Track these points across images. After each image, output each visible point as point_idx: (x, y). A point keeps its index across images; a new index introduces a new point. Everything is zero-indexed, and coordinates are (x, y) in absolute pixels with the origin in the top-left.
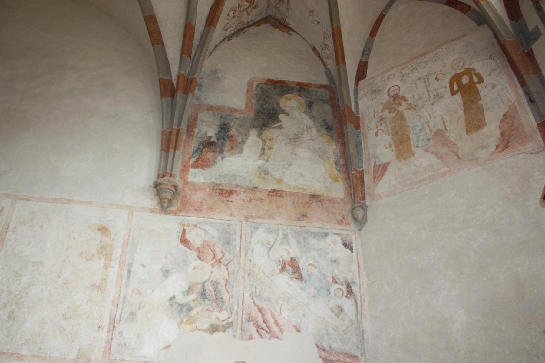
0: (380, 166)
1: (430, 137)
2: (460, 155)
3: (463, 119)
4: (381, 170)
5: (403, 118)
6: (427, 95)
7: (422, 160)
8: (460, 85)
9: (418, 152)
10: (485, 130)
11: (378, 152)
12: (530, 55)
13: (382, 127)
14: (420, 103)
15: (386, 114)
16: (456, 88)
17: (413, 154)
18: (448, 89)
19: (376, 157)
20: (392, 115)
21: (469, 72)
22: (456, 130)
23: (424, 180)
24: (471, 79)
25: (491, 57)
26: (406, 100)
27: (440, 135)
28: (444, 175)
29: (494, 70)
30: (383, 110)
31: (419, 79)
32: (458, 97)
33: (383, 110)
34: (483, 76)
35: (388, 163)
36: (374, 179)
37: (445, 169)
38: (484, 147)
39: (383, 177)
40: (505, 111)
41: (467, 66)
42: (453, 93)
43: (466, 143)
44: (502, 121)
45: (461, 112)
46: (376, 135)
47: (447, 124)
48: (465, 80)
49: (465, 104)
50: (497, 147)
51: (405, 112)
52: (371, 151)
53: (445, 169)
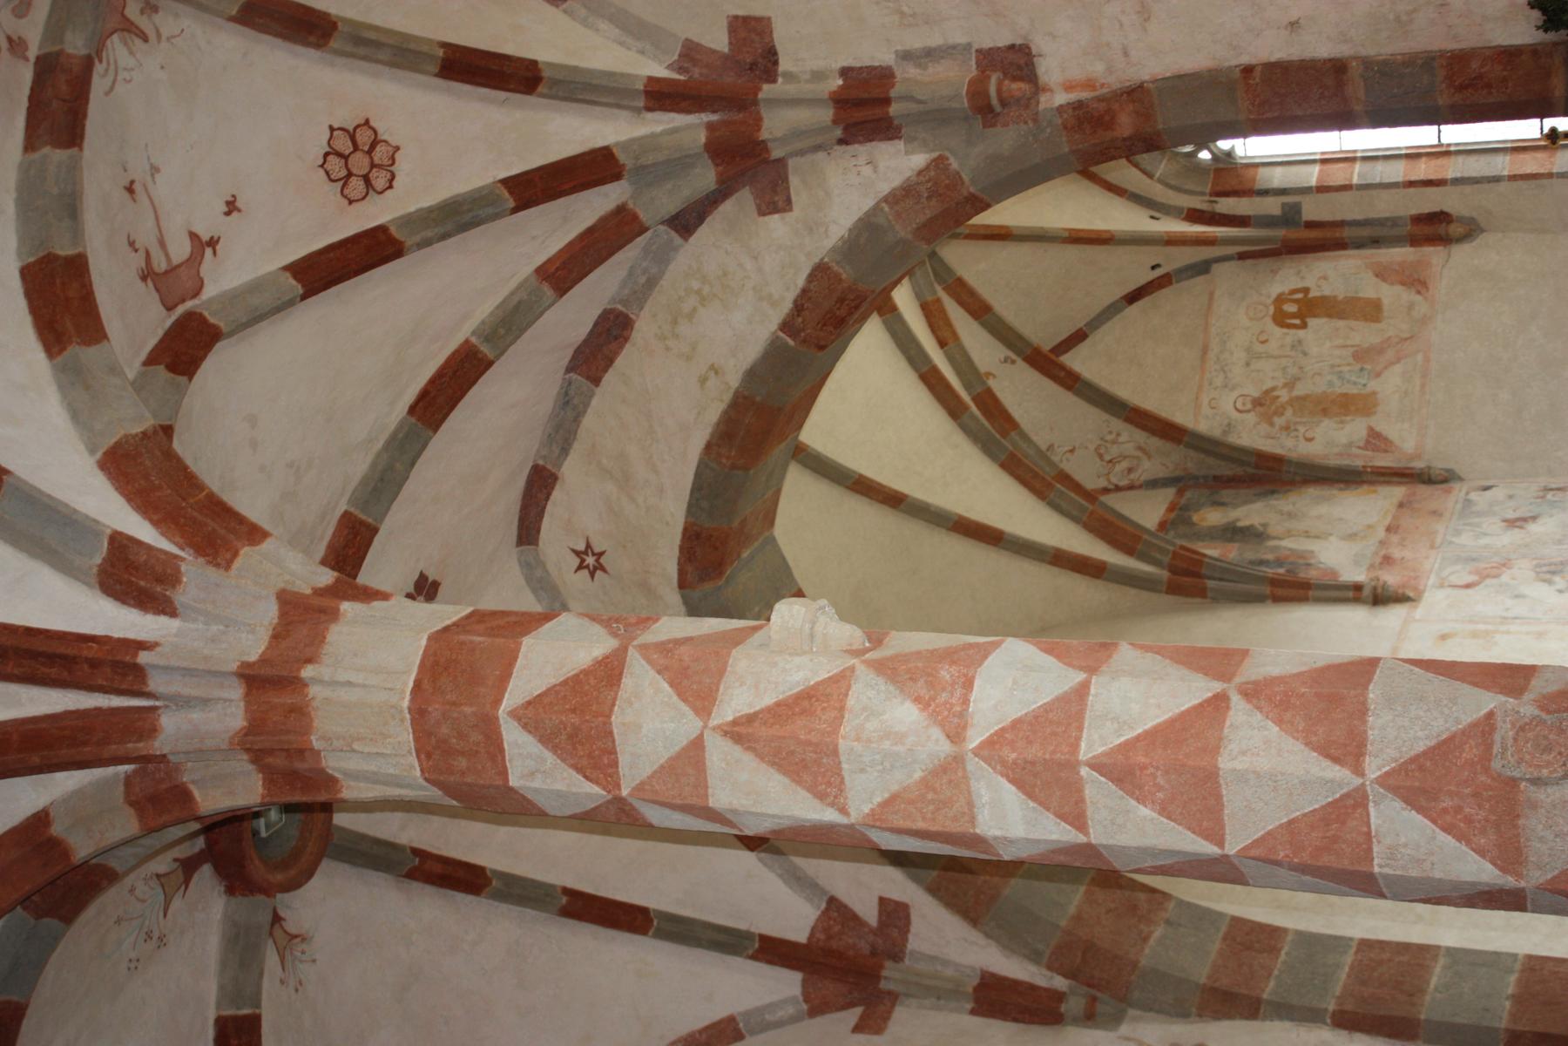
0: (1368, 442)
1: (1359, 366)
2: (1406, 335)
3: (1353, 323)
4: (1376, 440)
5: (1304, 398)
6: (1284, 361)
7: (1390, 385)
8: (1294, 316)
9: (1373, 385)
10: (1386, 302)
11: (1344, 440)
12: (1311, 225)
13: (1302, 429)
14: (1293, 371)
16: (1297, 322)
17: (1374, 393)
18: (1293, 331)
19: (1350, 445)
20: (1289, 412)
21: (1280, 300)
22: (1363, 334)
23: (1423, 386)
24: (1296, 301)
25: (1274, 272)
26: (1273, 389)
28: (1427, 360)
29: (1299, 272)
30: (1272, 424)
31: (1248, 364)
32: (1313, 322)
33: (1272, 424)
34: (1300, 285)
35: (1371, 429)
36: (1386, 451)
37: (1420, 357)
38: (1411, 307)
39: (1390, 437)
40: (1370, 274)
41: (1269, 301)
42: (1304, 326)
43: (1392, 326)
44: (1384, 280)
45: (1341, 323)
47: (1349, 342)
48: (1291, 308)
49: (1330, 316)
50: (1419, 292)
51: (1296, 393)
52: (1336, 450)
53: (1420, 357)
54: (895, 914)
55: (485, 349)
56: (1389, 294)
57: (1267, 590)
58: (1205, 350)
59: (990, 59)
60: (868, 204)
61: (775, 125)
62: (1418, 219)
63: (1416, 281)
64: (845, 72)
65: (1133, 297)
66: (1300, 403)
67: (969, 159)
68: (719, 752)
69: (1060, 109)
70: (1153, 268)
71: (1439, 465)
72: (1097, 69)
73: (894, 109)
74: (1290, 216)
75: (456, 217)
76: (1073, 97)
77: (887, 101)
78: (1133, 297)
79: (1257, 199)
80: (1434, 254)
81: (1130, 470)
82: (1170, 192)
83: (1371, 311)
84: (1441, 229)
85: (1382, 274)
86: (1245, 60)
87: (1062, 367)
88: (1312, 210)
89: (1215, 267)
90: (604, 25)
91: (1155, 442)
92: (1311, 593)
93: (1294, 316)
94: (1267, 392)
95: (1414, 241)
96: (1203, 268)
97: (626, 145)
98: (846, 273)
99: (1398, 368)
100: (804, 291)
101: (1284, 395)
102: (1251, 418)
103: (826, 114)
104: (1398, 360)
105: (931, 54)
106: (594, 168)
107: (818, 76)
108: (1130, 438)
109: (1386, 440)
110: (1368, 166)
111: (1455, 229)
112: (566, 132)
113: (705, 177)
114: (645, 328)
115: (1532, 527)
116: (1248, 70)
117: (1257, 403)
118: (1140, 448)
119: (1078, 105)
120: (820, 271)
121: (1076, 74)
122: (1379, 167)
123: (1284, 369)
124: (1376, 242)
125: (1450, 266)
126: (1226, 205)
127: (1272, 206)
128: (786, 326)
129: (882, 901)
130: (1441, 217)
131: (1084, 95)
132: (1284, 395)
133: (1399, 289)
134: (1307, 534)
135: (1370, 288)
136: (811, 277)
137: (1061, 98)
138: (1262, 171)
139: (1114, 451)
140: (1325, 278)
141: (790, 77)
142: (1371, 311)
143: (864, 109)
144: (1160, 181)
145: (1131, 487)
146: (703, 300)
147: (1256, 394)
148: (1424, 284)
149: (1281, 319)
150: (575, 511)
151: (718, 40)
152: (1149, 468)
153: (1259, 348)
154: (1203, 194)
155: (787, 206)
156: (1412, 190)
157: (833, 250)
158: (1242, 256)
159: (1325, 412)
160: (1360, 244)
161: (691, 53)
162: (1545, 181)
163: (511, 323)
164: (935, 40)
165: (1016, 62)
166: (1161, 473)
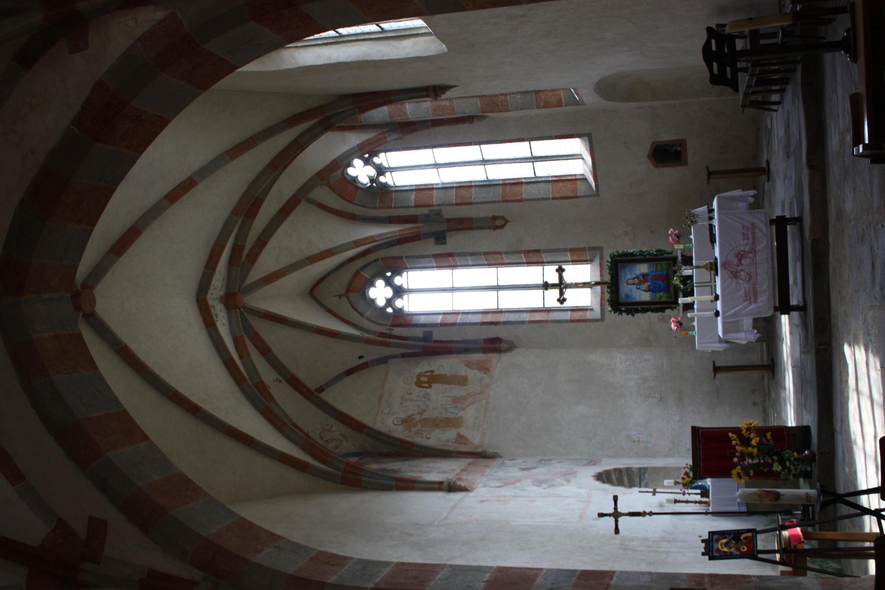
3: (453, 386)
4: (461, 439)
7: (469, 414)
8: (426, 382)
9: (461, 414)
10: (469, 377)
12: (436, 341)
13: (425, 433)
15: (414, 430)
17: (461, 417)
18: (424, 390)
19: (448, 441)
20: (419, 426)
21: (419, 375)
22: (458, 391)
23: (485, 414)
24: (427, 376)
26: (413, 415)
27: (456, 400)
28: (488, 403)
30: (410, 431)
32: (434, 386)
33: (410, 431)
34: (430, 369)
37: (484, 401)
38: (481, 379)
42: (430, 387)
44: (470, 368)
45: (448, 386)
46: (428, 438)
48: (425, 379)
49: (443, 383)
53: (484, 401)
54: (98, 527)
56: (471, 374)
57: (394, 483)
58: (381, 397)
62: (487, 341)
63: (485, 368)
65: (349, 372)
66: (424, 422)
70: (361, 357)
71: (490, 450)
74: (427, 337)
78: (349, 372)
79: (412, 329)
80: (493, 357)
81: (336, 447)
82: (371, 324)
83: (462, 381)
84: (497, 345)
85: (468, 365)
88: (438, 335)
89: (390, 361)
91: (349, 432)
92: (416, 485)
93: (426, 382)
94: (409, 417)
95: (485, 351)
96: (384, 360)
99: (474, 407)
101: (418, 418)
102: (400, 428)
104: (474, 403)
109: (466, 439)
110: (465, 316)
111: (504, 346)
115: (534, 471)
117: (404, 421)
118: (342, 435)
122: (470, 316)
123: (419, 406)
124: (467, 351)
125: (500, 362)
126: (397, 331)
127: (419, 332)
129: (91, 519)
130: (497, 340)
132: (418, 418)
133: (476, 372)
134: (421, 472)
135: (462, 371)
138: (415, 317)
140: (442, 366)
142: (462, 381)
144: (367, 318)
147: (404, 417)
148: (488, 370)
149: (419, 384)
153: (408, 396)
154: (387, 325)
156: (484, 326)
158: (404, 356)
159: (437, 426)
160: (459, 352)
162: (545, 324)
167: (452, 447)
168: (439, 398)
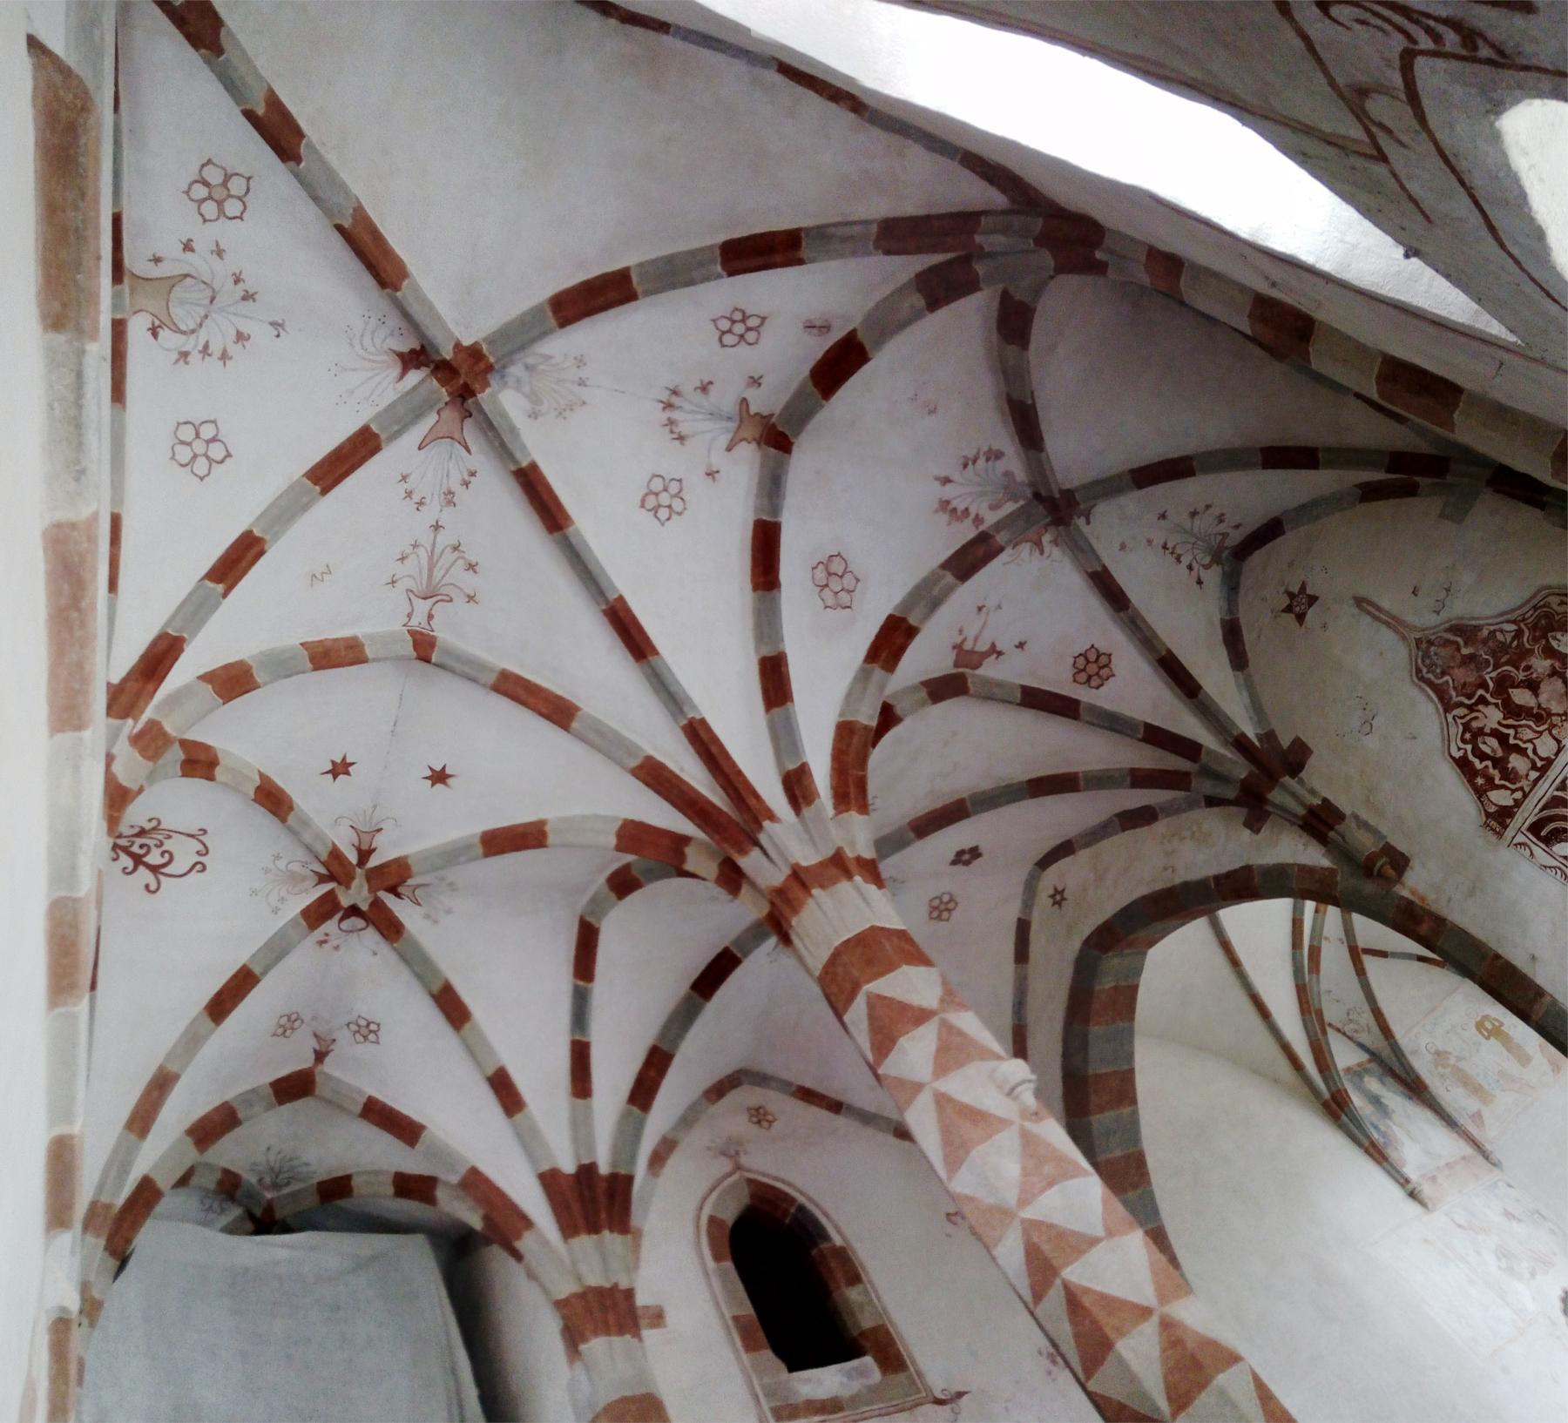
4: (1477, 1117)
5: (1460, 1070)
15: (1440, 1069)
22: (1512, 1066)
45: (1505, 1053)
48: (1489, 1026)
55: (1082, 783)
58: (1434, 1009)
59: (1389, 851)
60: (1290, 861)
61: (1277, 796)
64: (1325, 800)
66: (1457, 1071)
67: (1346, 881)
68: (925, 1100)
69: (1402, 898)
72: (1431, 897)
73: (1332, 834)
75: (1113, 723)
76: (1411, 897)
77: (1332, 829)
83: (1524, 1060)
86: (1500, 951)
87: (1361, 963)
90: (1245, 694)
91: (1376, 1029)
97: (1210, 752)
98: (1257, 880)
100: (1235, 871)
101: (1452, 1061)
102: (1429, 1057)
103: (1301, 811)
105: (1366, 826)
106: (1190, 749)
107: (1313, 792)
108: (1367, 1018)
112: (1189, 726)
113: (1231, 793)
114: (1160, 826)
116: (1498, 957)
117: (1438, 1053)
119: (1411, 903)
120: (1247, 869)
121: (1422, 889)
128: (1217, 878)
131: (1417, 901)
136: (1242, 868)
137: (1405, 893)
139: (1353, 1016)
141: (1301, 782)
142: (1524, 1060)
143: (1320, 822)
145: (1350, 1038)
146: (1192, 837)
148: (1559, 1069)
149: (1480, 1026)
150: (1068, 872)
151: (1285, 742)
152: (1364, 1038)
155: (1257, 831)
157: (1261, 866)
161: (1269, 737)
163: (1101, 781)
164: (1372, 822)
165: (1400, 862)
166: (1368, 1043)
167: (1463, 1120)
168: (1487, 1058)
